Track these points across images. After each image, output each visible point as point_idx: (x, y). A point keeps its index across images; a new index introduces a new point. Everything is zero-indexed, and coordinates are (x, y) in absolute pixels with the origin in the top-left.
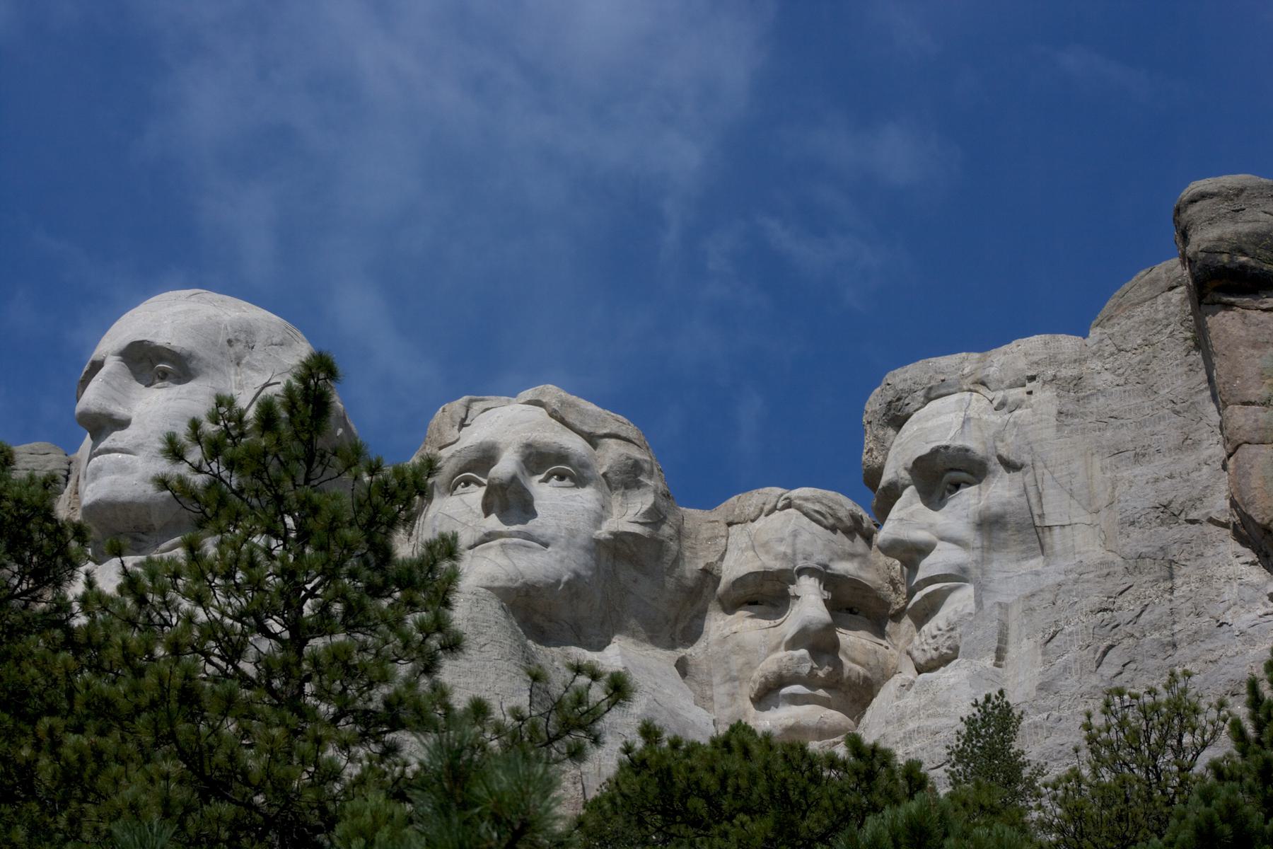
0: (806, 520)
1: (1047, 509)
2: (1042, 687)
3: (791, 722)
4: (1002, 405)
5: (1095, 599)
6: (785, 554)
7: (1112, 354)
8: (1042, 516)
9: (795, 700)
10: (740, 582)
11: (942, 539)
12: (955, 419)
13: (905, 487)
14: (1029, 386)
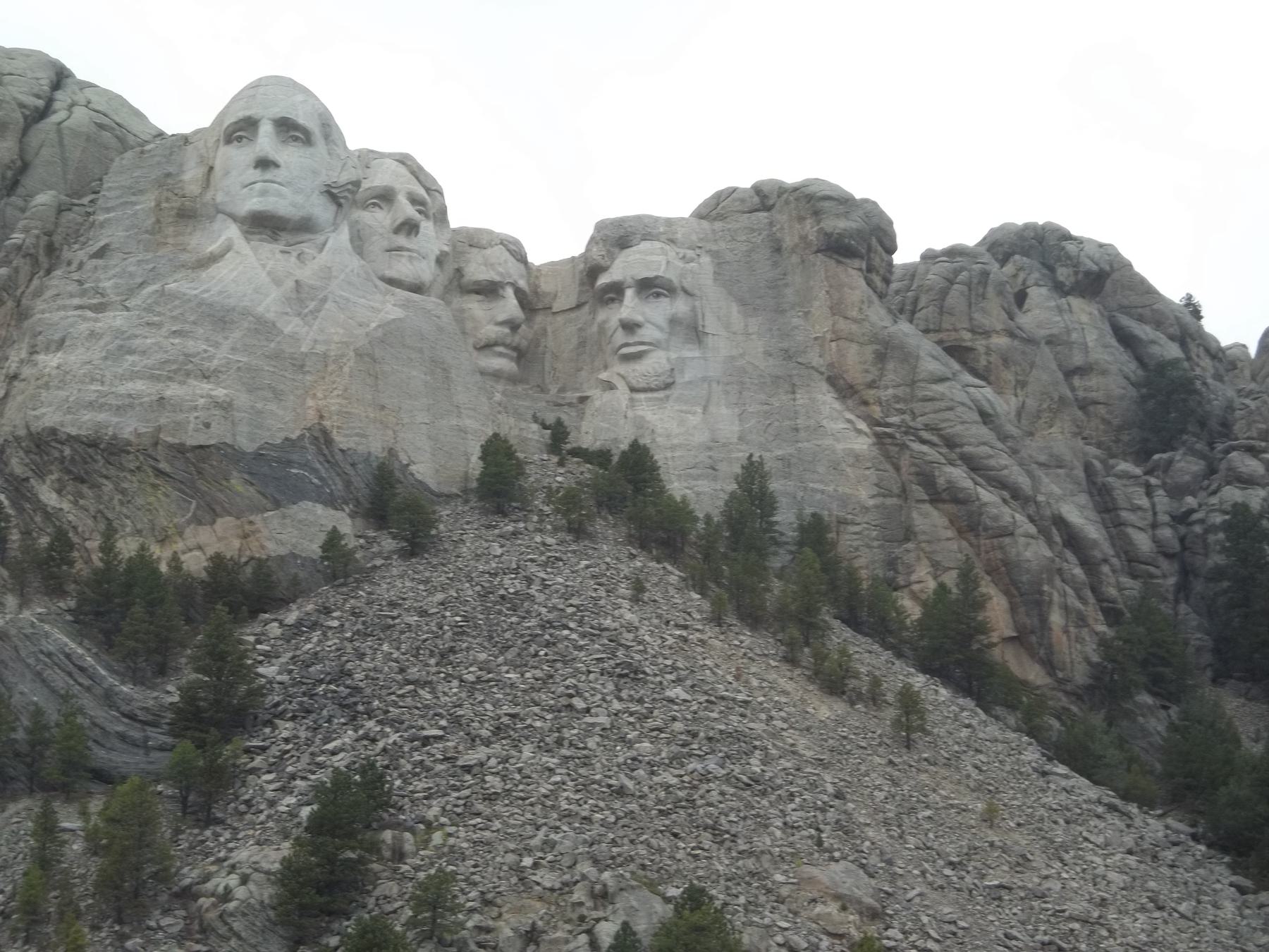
0: (507, 254)
1: (707, 323)
2: (740, 439)
3: (497, 367)
4: (684, 257)
5: (763, 397)
9: (501, 355)
10: (477, 283)
12: (662, 258)
14: (698, 251)
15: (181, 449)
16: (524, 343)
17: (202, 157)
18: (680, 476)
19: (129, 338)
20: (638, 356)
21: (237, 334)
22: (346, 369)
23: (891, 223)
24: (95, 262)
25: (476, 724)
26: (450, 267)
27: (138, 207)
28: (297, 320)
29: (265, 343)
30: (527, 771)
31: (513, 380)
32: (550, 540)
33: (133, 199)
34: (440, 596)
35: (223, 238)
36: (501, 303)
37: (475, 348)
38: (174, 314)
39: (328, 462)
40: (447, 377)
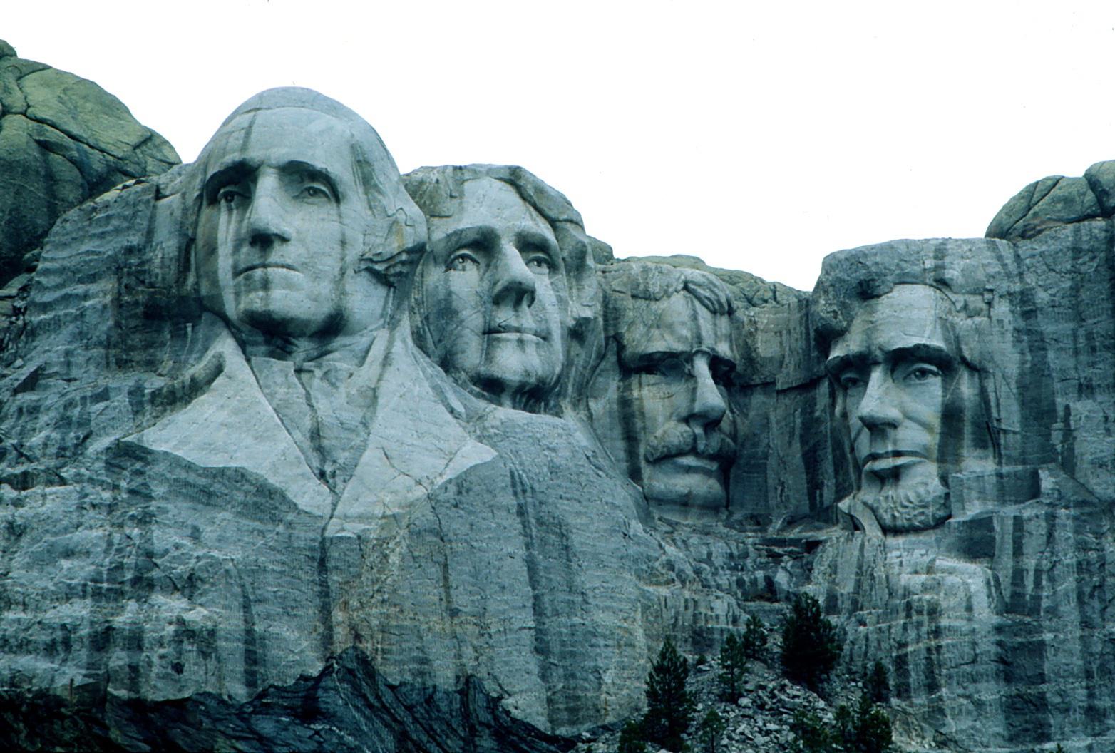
1: (1003, 414)
6: (687, 338)
7: (1044, 272)
8: (999, 420)
9: (688, 470)
11: (910, 418)
13: (876, 363)
14: (987, 296)
15: (139, 709)
18: (950, 677)
19: (66, 530)
20: (895, 475)
21: (227, 515)
22: (394, 559)
24: (19, 396)
26: (597, 339)
27: (87, 304)
28: (315, 483)
29: (270, 527)
31: (711, 507)
33: (80, 289)
35: (211, 353)
37: (648, 461)
38: (134, 485)
39: (370, 706)
40: (567, 548)
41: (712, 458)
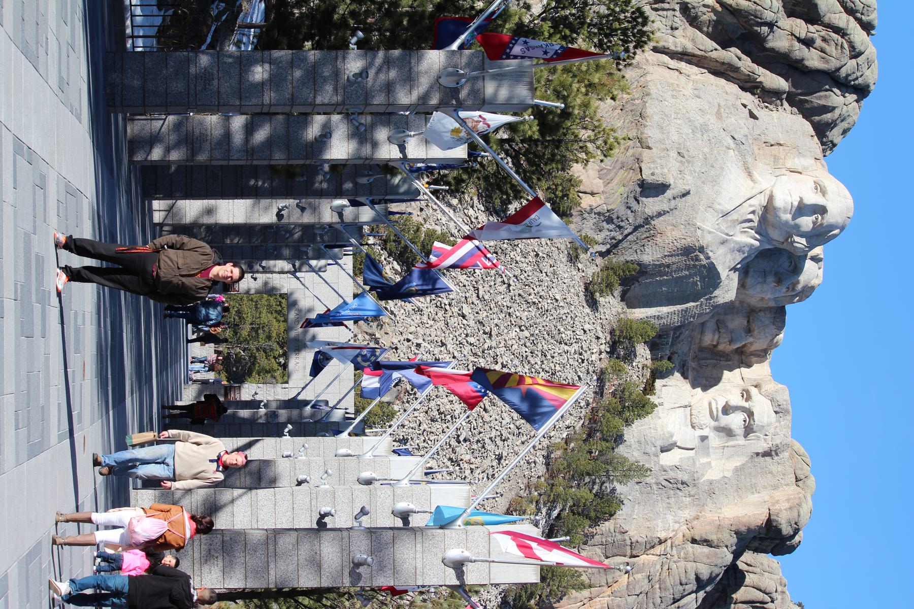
2: (662, 466)
5: (685, 478)
9: (714, 335)
14: (771, 443)
16: (721, 347)
17: (808, 168)
23: (790, 552)
25: (485, 314)
26: (760, 305)
30: (460, 339)
32: (594, 356)
34: (558, 297)
36: (743, 334)
41: (718, 343)
